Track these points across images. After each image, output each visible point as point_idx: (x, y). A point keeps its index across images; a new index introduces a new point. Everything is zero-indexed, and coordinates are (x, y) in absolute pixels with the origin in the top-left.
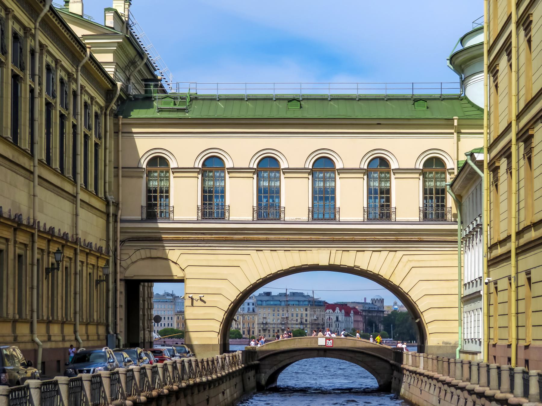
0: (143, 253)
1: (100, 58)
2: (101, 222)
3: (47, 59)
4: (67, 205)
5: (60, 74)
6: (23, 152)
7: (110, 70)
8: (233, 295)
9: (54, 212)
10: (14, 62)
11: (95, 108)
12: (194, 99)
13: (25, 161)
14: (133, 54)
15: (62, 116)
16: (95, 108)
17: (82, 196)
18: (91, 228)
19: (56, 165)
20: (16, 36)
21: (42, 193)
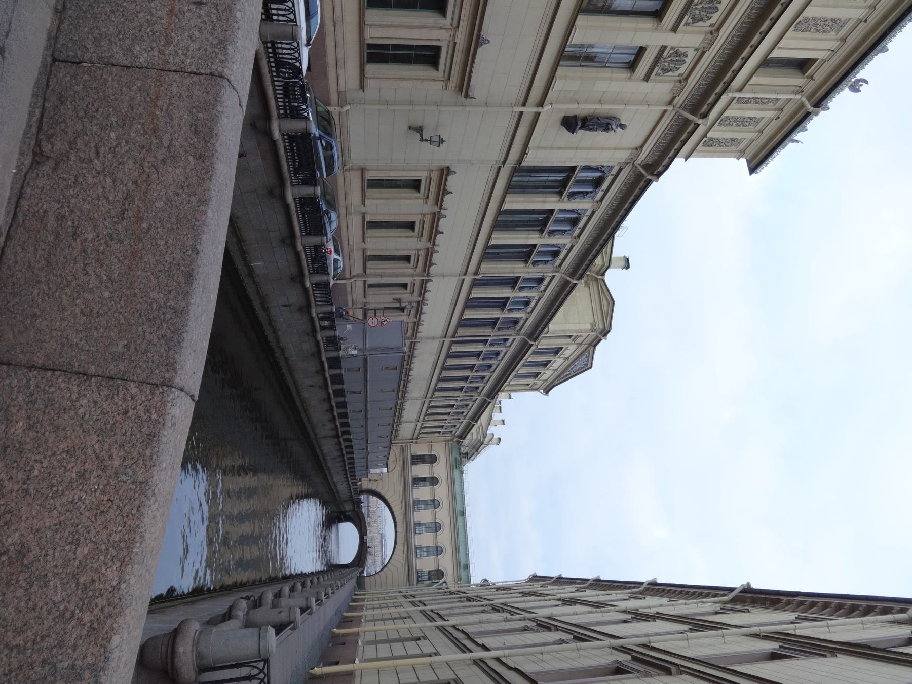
0: (398, 455)
1: (473, 430)
2: (409, 436)
3: (470, 403)
4: (414, 417)
5: (466, 411)
6: (433, 394)
7: (469, 437)
8: (383, 493)
9: (411, 410)
10: (468, 388)
11: (454, 430)
12: (461, 472)
13: (429, 395)
14: (477, 448)
15: (449, 413)
16: (454, 430)
17: (419, 424)
18: (406, 430)
19: (430, 411)
20: (477, 388)
21: (419, 402)
